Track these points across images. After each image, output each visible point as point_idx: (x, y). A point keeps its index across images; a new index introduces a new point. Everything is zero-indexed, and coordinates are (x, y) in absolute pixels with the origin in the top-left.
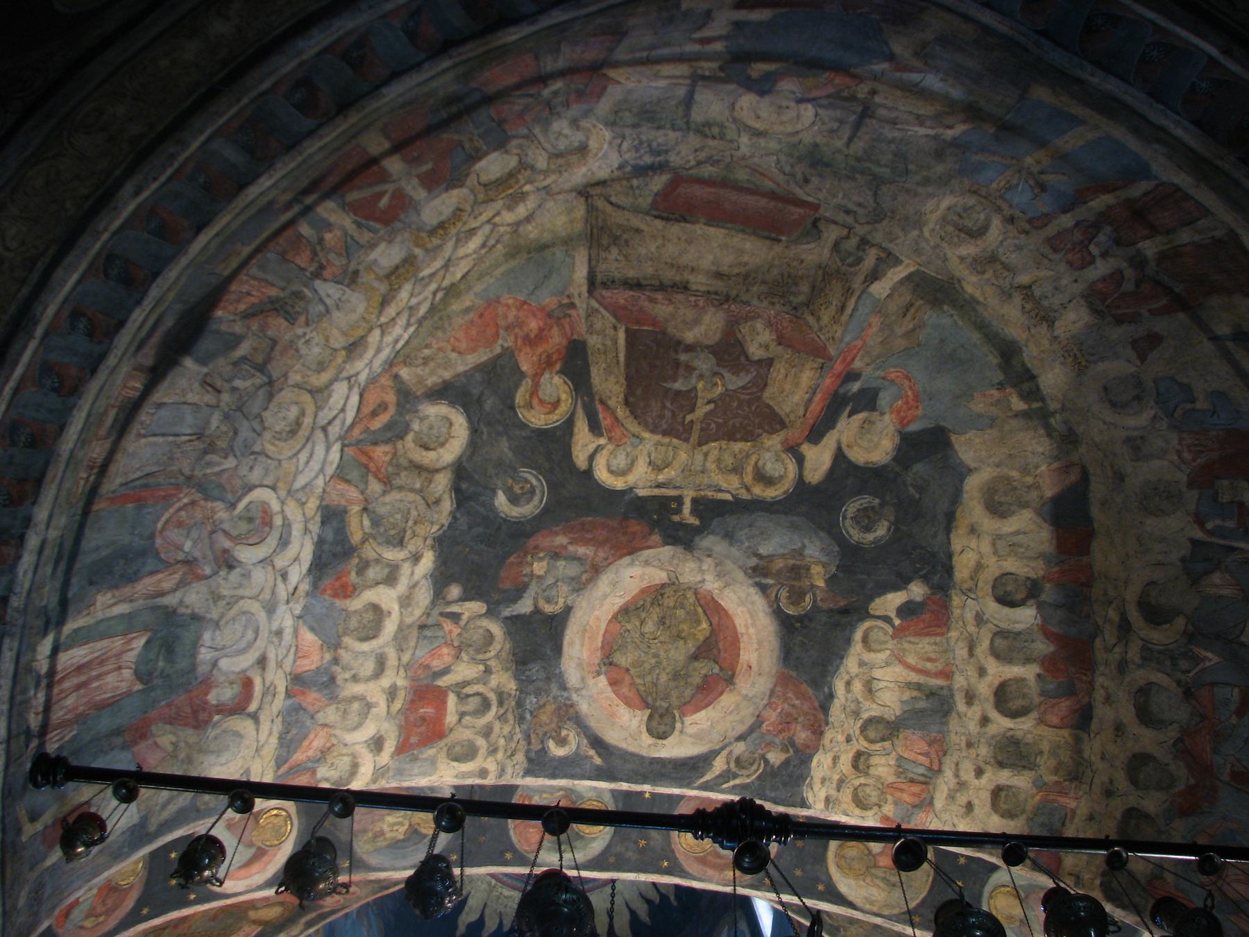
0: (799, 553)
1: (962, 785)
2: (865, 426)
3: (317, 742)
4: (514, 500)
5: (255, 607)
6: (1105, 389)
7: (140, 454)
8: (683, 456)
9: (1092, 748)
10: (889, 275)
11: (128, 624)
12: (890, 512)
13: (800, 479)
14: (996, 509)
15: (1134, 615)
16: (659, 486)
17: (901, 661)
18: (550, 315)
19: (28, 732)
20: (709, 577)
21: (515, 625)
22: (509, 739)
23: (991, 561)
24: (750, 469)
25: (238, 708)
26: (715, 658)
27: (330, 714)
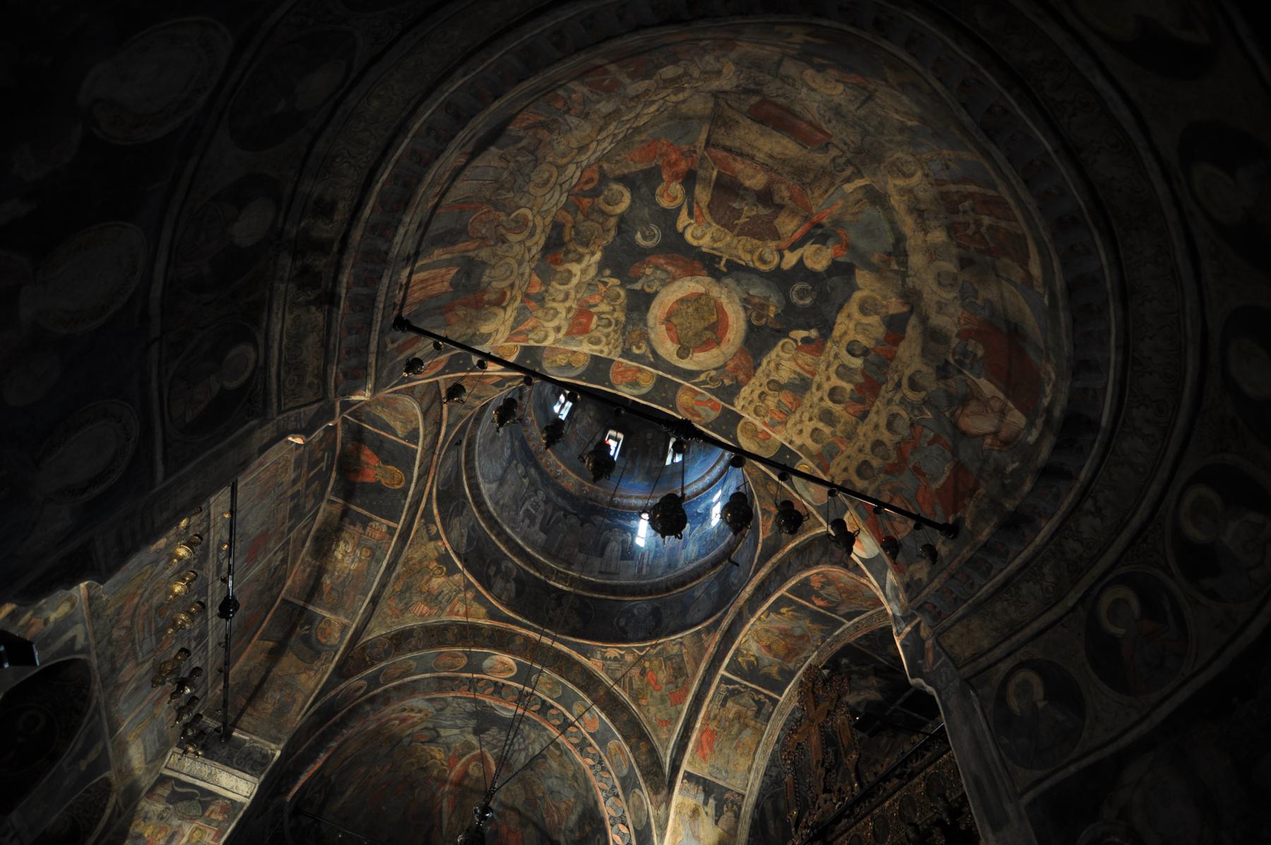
0: (767, 299)
1: (801, 421)
2: (816, 253)
3: (530, 323)
4: (645, 238)
5: (513, 261)
7: (463, 188)
9: (862, 429)
11: (449, 263)
12: (814, 294)
13: (778, 267)
14: (864, 310)
15: (905, 382)
17: (795, 360)
18: (683, 154)
19: (395, 304)
21: (632, 294)
22: (617, 340)
23: (852, 333)
25: (500, 302)
26: (714, 333)
27: (540, 313)
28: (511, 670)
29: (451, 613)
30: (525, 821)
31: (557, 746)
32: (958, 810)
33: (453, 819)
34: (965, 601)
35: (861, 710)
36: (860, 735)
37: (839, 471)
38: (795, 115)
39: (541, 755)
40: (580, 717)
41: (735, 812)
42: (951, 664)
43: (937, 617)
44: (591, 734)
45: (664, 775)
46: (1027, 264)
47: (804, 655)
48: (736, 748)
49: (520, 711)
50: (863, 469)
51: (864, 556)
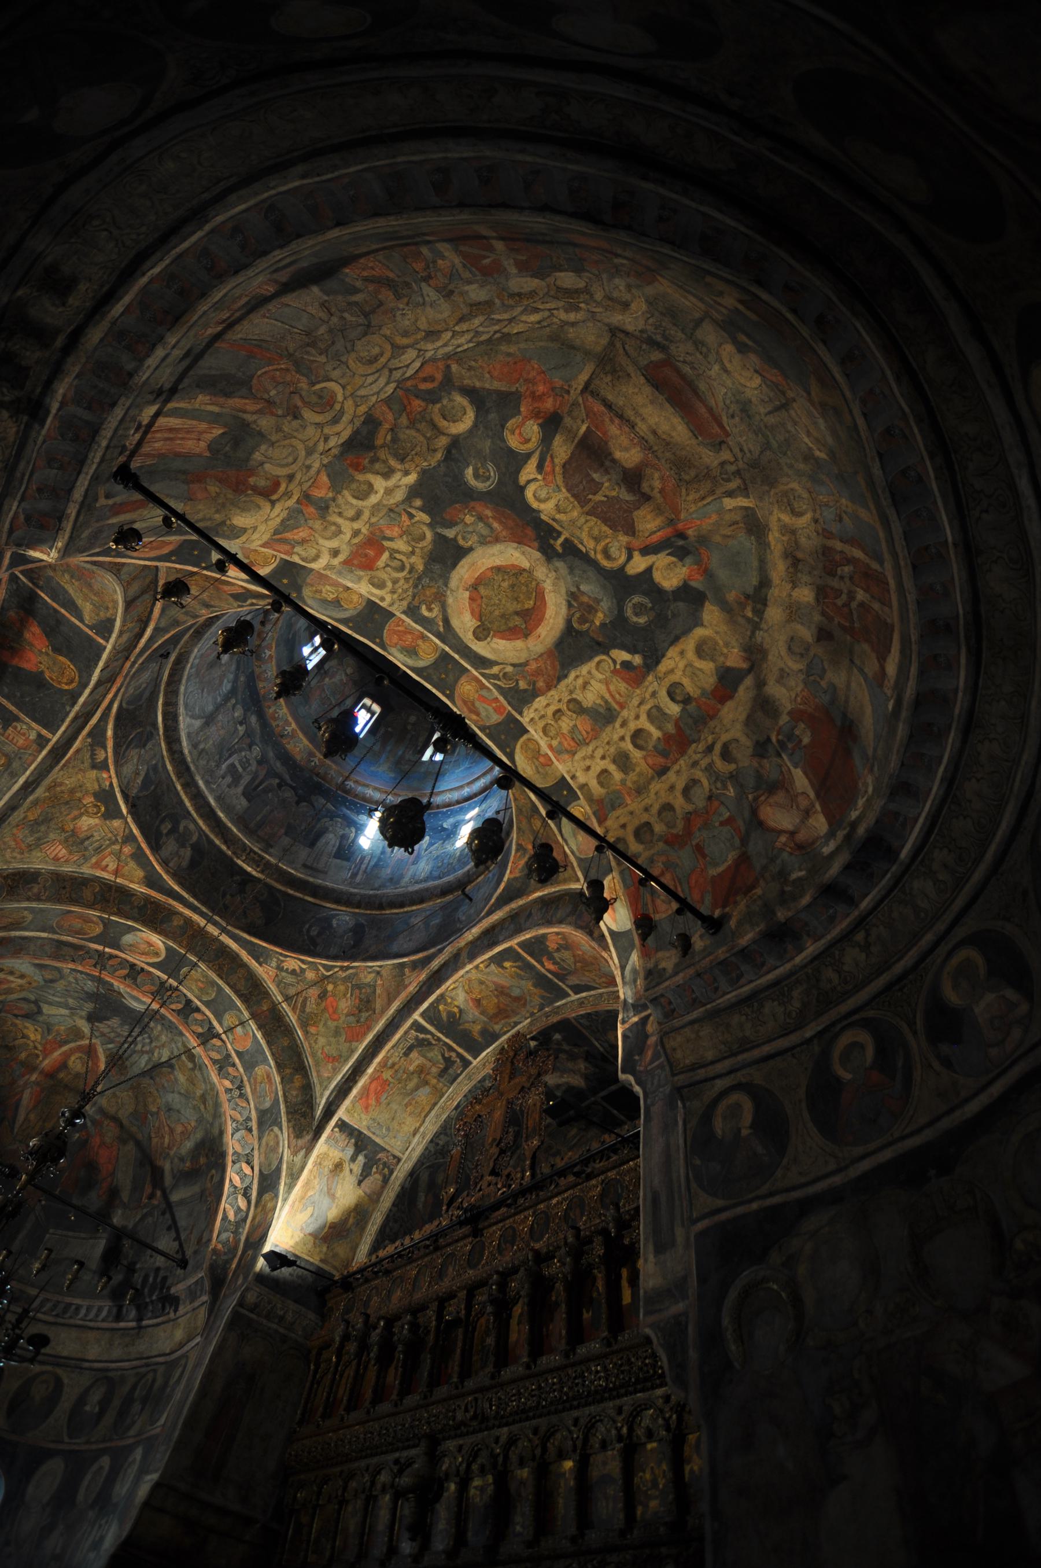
0: (598, 601)
2: (669, 567)
6: (792, 638)
8: (575, 514)
10: (739, 499)
13: (622, 568)
16: (554, 520)
20: (548, 581)
21: (440, 540)
24: (603, 544)
26: (525, 622)
28: (157, 954)
29: (97, 865)
30: (125, 1136)
31: (192, 1057)
32: (626, 1223)
33: (32, 1116)
34: (705, 1005)
35: (559, 1094)
36: (549, 1120)
37: (616, 826)
38: (695, 391)
39: (169, 1064)
40: (230, 1030)
41: (384, 1176)
42: (667, 1068)
43: (669, 1014)
44: (238, 1053)
45: (313, 1117)
46: (885, 660)
47: (515, 1019)
48: (406, 1106)
49: (155, 1006)
50: (643, 832)
51: (614, 927)
